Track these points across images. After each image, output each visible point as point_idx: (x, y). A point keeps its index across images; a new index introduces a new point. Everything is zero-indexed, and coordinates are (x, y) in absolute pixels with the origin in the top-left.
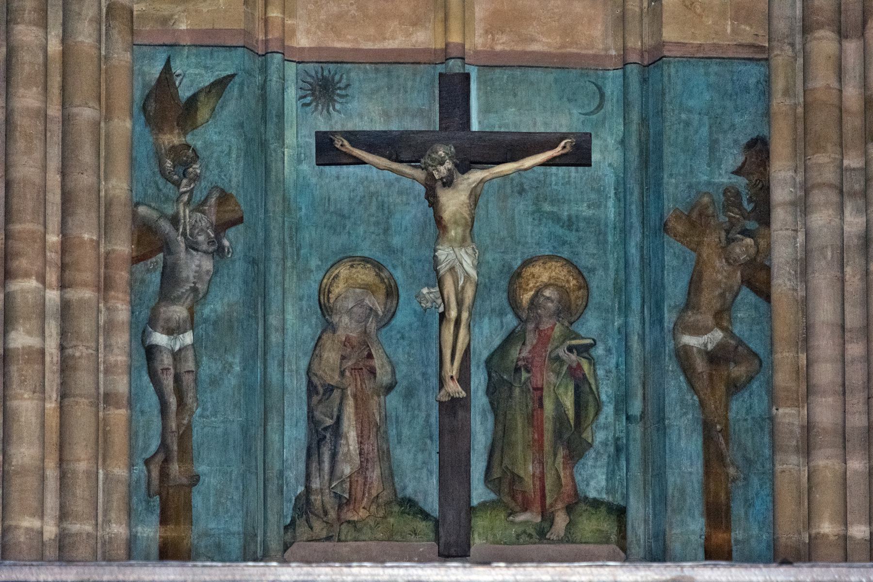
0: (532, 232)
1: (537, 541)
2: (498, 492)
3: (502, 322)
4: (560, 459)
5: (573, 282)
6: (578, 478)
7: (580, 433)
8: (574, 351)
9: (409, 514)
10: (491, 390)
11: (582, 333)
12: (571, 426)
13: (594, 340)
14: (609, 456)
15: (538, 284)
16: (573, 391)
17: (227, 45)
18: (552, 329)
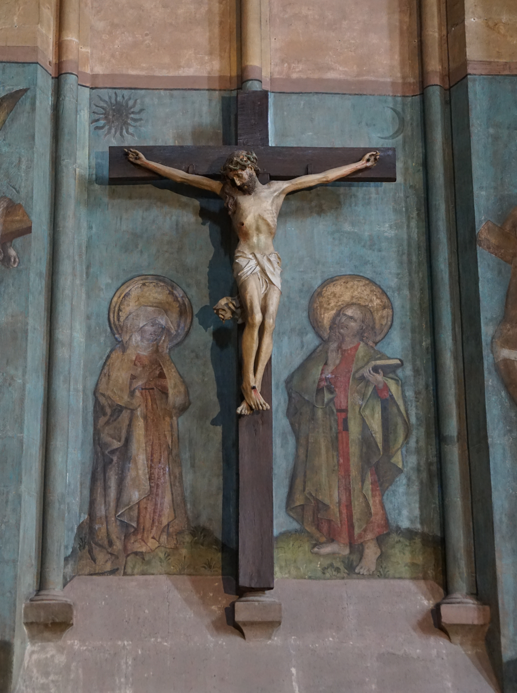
0: (332, 251)
1: (345, 575)
2: (301, 520)
3: (302, 342)
4: (368, 485)
5: (376, 302)
6: (388, 506)
7: (390, 457)
8: (380, 371)
9: (202, 545)
11: (388, 352)
12: (379, 449)
13: (400, 360)
14: (421, 483)
15: (340, 303)
16: (380, 413)
17: (19, 61)
18: (356, 348)
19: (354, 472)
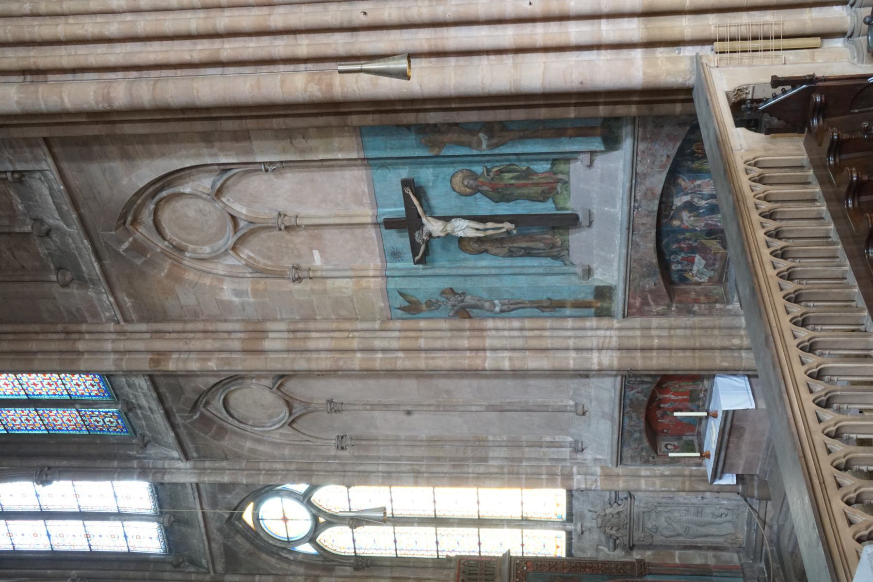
2: (548, 198)
4: (535, 177)
6: (542, 171)
10: (507, 200)
19: (530, 182)
